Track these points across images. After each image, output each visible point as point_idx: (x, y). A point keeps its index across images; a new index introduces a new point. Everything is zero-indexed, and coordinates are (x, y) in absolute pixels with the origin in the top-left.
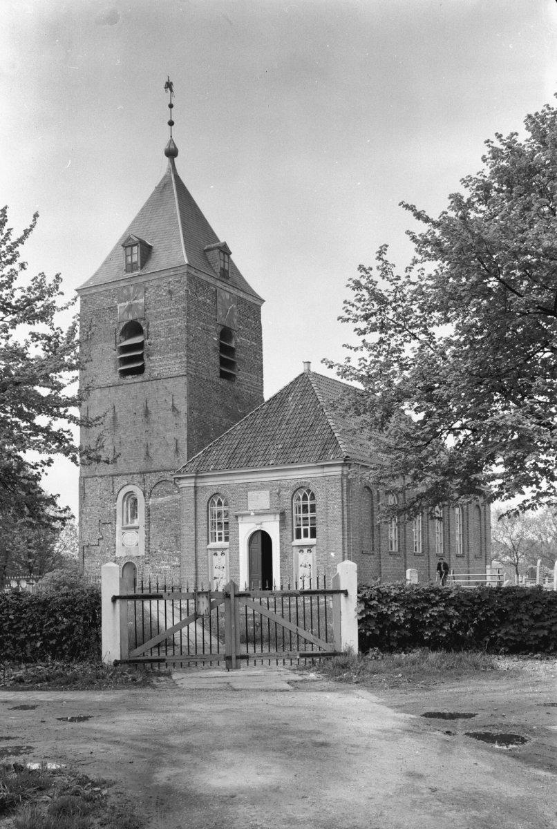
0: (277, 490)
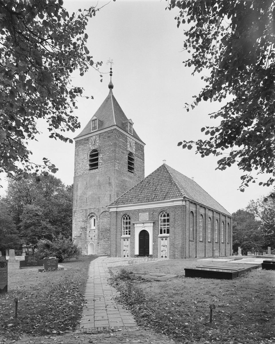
0: (152, 212)
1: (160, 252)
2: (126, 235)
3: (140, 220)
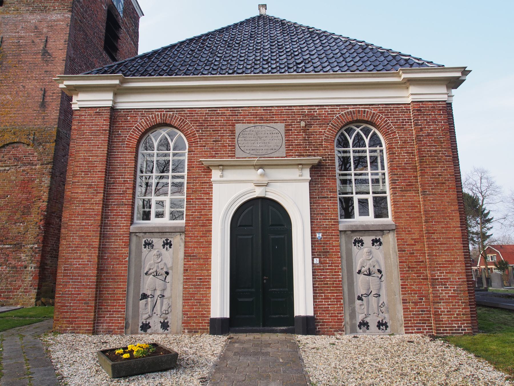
0: (303, 124)
1: (352, 302)
3: (239, 153)
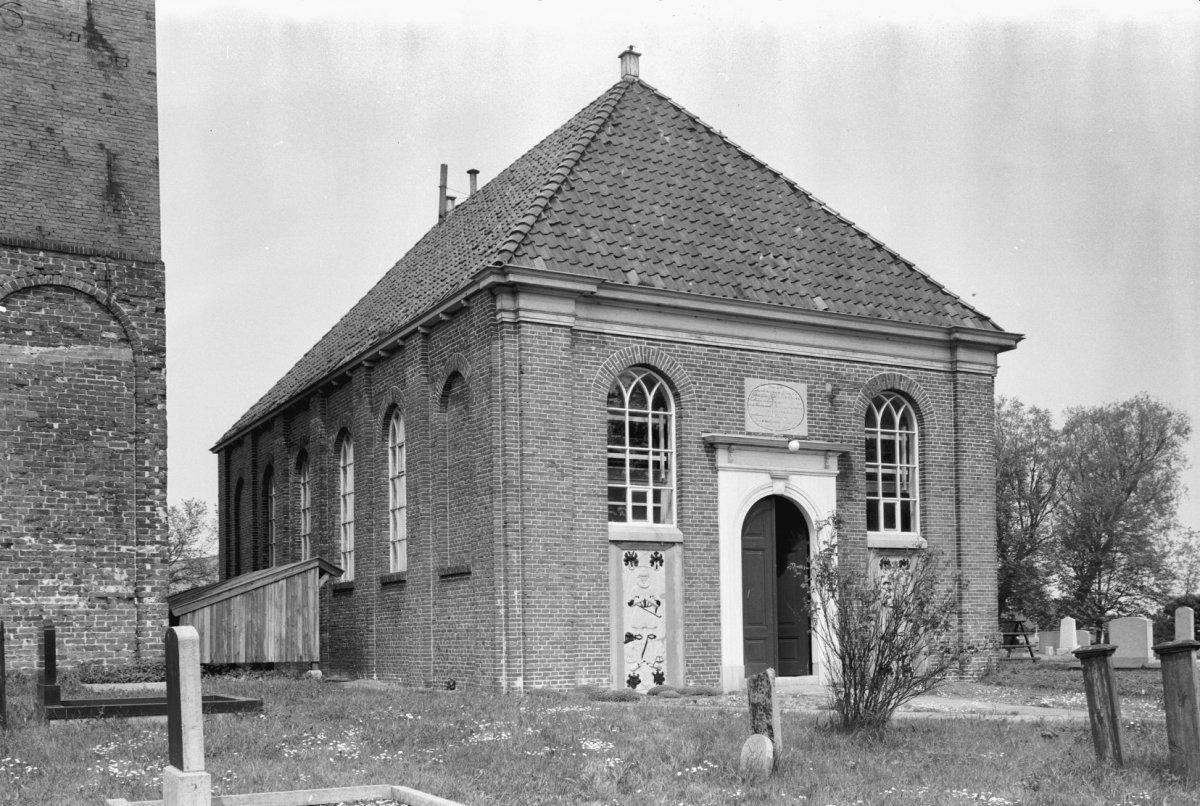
0: (829, 387)
2: (640, 523)
